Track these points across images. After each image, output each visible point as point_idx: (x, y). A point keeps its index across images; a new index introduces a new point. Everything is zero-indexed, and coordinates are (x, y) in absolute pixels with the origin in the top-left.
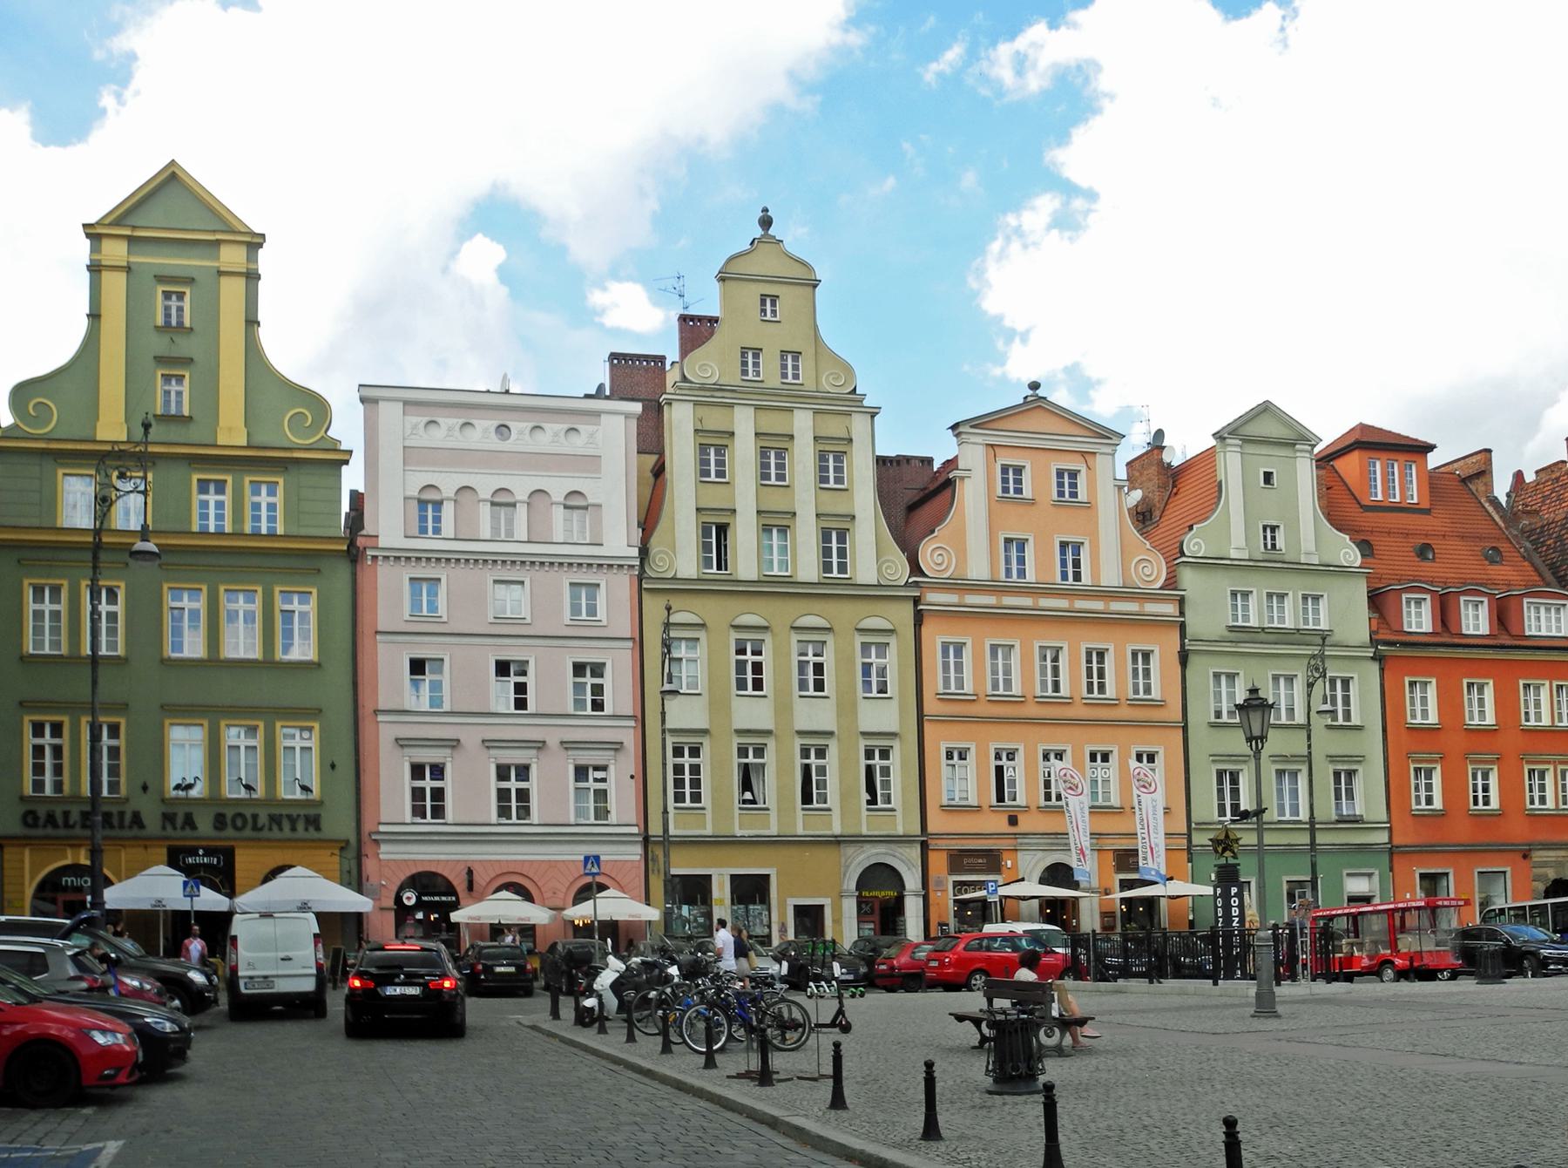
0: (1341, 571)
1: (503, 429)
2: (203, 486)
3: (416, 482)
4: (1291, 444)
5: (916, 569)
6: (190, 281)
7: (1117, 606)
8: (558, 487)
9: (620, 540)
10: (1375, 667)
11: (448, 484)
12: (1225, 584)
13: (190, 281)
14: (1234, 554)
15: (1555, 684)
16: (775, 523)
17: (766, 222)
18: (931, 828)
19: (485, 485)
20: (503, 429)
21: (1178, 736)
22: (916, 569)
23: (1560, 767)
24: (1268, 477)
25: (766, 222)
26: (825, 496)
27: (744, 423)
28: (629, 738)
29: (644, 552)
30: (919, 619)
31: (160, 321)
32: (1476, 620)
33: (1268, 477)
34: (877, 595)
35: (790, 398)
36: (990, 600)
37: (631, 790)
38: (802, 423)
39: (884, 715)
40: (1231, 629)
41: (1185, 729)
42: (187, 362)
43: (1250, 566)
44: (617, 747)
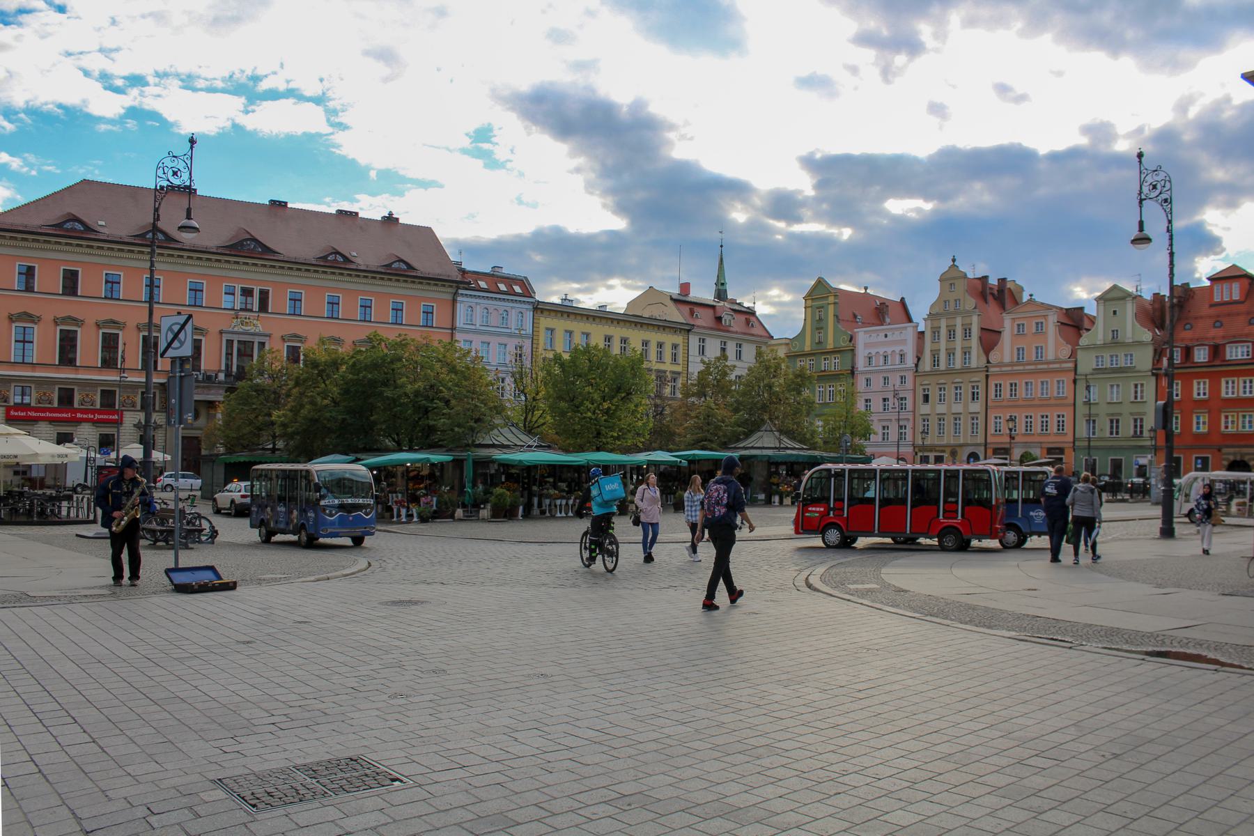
0: (1140, 344)
1: (886, 336)
2: (825, 359)
3: (867, 351)
4: (1123, 298)
5: (988, 362)
6: (822, 307)
7: (1051, 366)
8: (897, 349)
9: (910, 361)
10: (1153, 379)
11: (873, 352)
12: (1093, 355)
13: (822, 307)
14: (1098, 343)
15: (1241, 379)
16: (950, 353)
17: (954, 260)
18: (988, 441)
19: (881, 351)
20: (886, 336)
21: (1072, 407)
22: (988, 362)
23: (1240, 414)
24: (1115, 312)
25: (954, 260)
26: (965, 342)
27: (943, 324)
28: (911, 418)
29: (917, 365)
30: (987, 377)
31: (818, 318)
32: (1201, 355)
33: (1115, 312)
34: (976, 371)
35: (956, 313)
36: (1009, 368)
37: (911, 430)
38: (959, 321)
39: (976, 407)
40: (1094, 370)
41: (1074, 404)
42: (822, 328)
43: (1105, 346)
44: (908, 420)
